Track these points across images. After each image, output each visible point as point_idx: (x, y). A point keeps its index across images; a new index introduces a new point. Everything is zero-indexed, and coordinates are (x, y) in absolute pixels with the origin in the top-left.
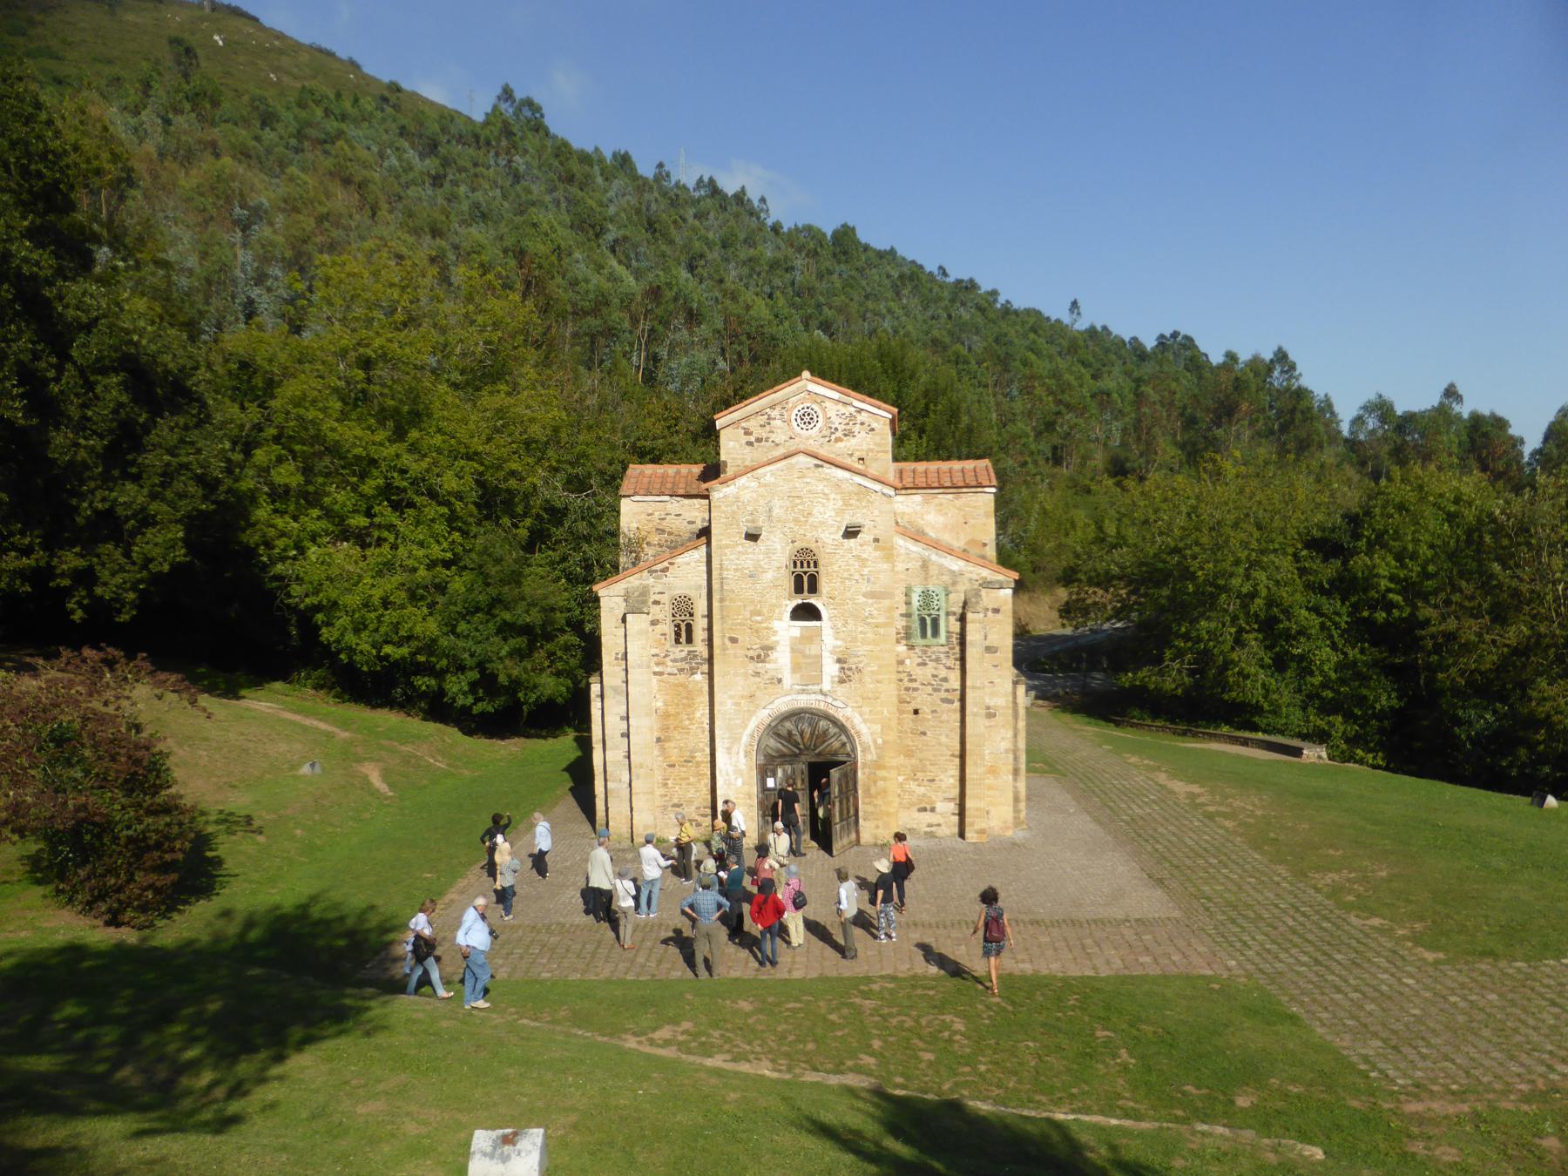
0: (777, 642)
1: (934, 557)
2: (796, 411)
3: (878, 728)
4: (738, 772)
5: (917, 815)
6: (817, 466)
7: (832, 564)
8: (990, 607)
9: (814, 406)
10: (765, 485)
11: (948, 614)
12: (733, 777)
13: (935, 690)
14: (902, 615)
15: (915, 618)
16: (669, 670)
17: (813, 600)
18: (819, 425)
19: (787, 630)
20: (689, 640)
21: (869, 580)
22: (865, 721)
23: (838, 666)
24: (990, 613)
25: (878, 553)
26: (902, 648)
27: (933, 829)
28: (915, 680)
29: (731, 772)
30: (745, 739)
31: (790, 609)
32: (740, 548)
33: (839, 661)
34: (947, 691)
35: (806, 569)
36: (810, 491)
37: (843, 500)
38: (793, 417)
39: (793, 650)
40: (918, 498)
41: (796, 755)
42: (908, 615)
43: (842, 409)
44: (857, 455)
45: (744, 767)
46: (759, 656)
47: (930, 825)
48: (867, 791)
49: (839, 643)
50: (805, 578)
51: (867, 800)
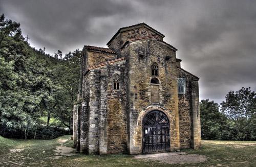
16: (112, 97)
17: (157, 77)
19: (150, 87)
20: (118, 88)
33: (164, 96)
43: (153, 33)
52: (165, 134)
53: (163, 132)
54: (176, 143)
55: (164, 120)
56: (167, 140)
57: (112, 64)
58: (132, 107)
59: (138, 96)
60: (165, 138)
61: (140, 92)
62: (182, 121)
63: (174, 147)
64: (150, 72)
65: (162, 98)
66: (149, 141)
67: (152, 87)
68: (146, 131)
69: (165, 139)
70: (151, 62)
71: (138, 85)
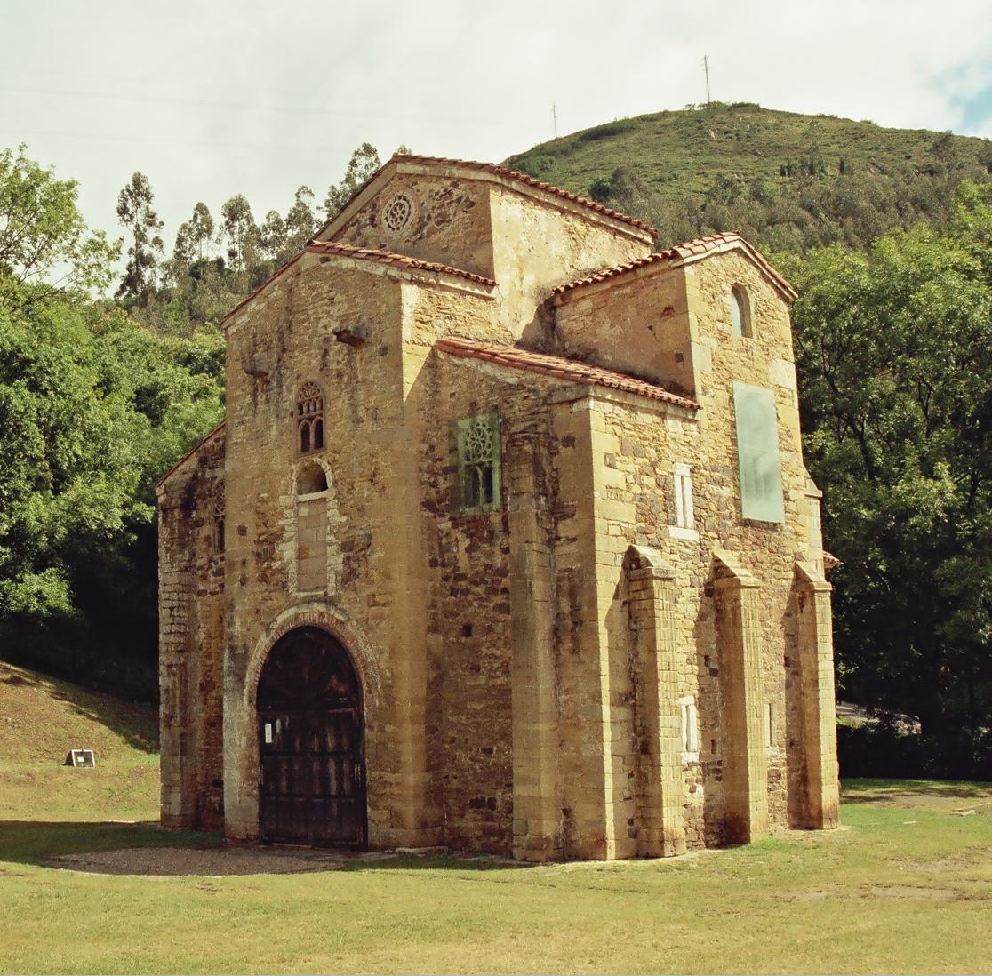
2: (387, 207)
8: (562, 435)
11: (503, 459)
12: (237, 733)
13: (493, 591)
16: (212, 587)
17: (316, 459)
18: (410, 220)
26: (445, 525)
28: (462, 577)
31: (294, 478)
34: (505, 591)
35: (313, 414)
38: (383, 217)
40: (586, 305)
42: (453, 469)
43: (437, 187)
46: (265, 550)
49: (344, 519)
50: (312, 430)
52: (338, 754)
53: (331, 742)
54: (398, 806)
56: (346, 785)
57: (211, 442)
58: (231, 624)
59: (252, 570)
61: (254, 548)
62: (482, 679)
63: (385, 828)
65: (336, 561)
67: (304, 511)
70: (295, 388)
71: (249, 520)
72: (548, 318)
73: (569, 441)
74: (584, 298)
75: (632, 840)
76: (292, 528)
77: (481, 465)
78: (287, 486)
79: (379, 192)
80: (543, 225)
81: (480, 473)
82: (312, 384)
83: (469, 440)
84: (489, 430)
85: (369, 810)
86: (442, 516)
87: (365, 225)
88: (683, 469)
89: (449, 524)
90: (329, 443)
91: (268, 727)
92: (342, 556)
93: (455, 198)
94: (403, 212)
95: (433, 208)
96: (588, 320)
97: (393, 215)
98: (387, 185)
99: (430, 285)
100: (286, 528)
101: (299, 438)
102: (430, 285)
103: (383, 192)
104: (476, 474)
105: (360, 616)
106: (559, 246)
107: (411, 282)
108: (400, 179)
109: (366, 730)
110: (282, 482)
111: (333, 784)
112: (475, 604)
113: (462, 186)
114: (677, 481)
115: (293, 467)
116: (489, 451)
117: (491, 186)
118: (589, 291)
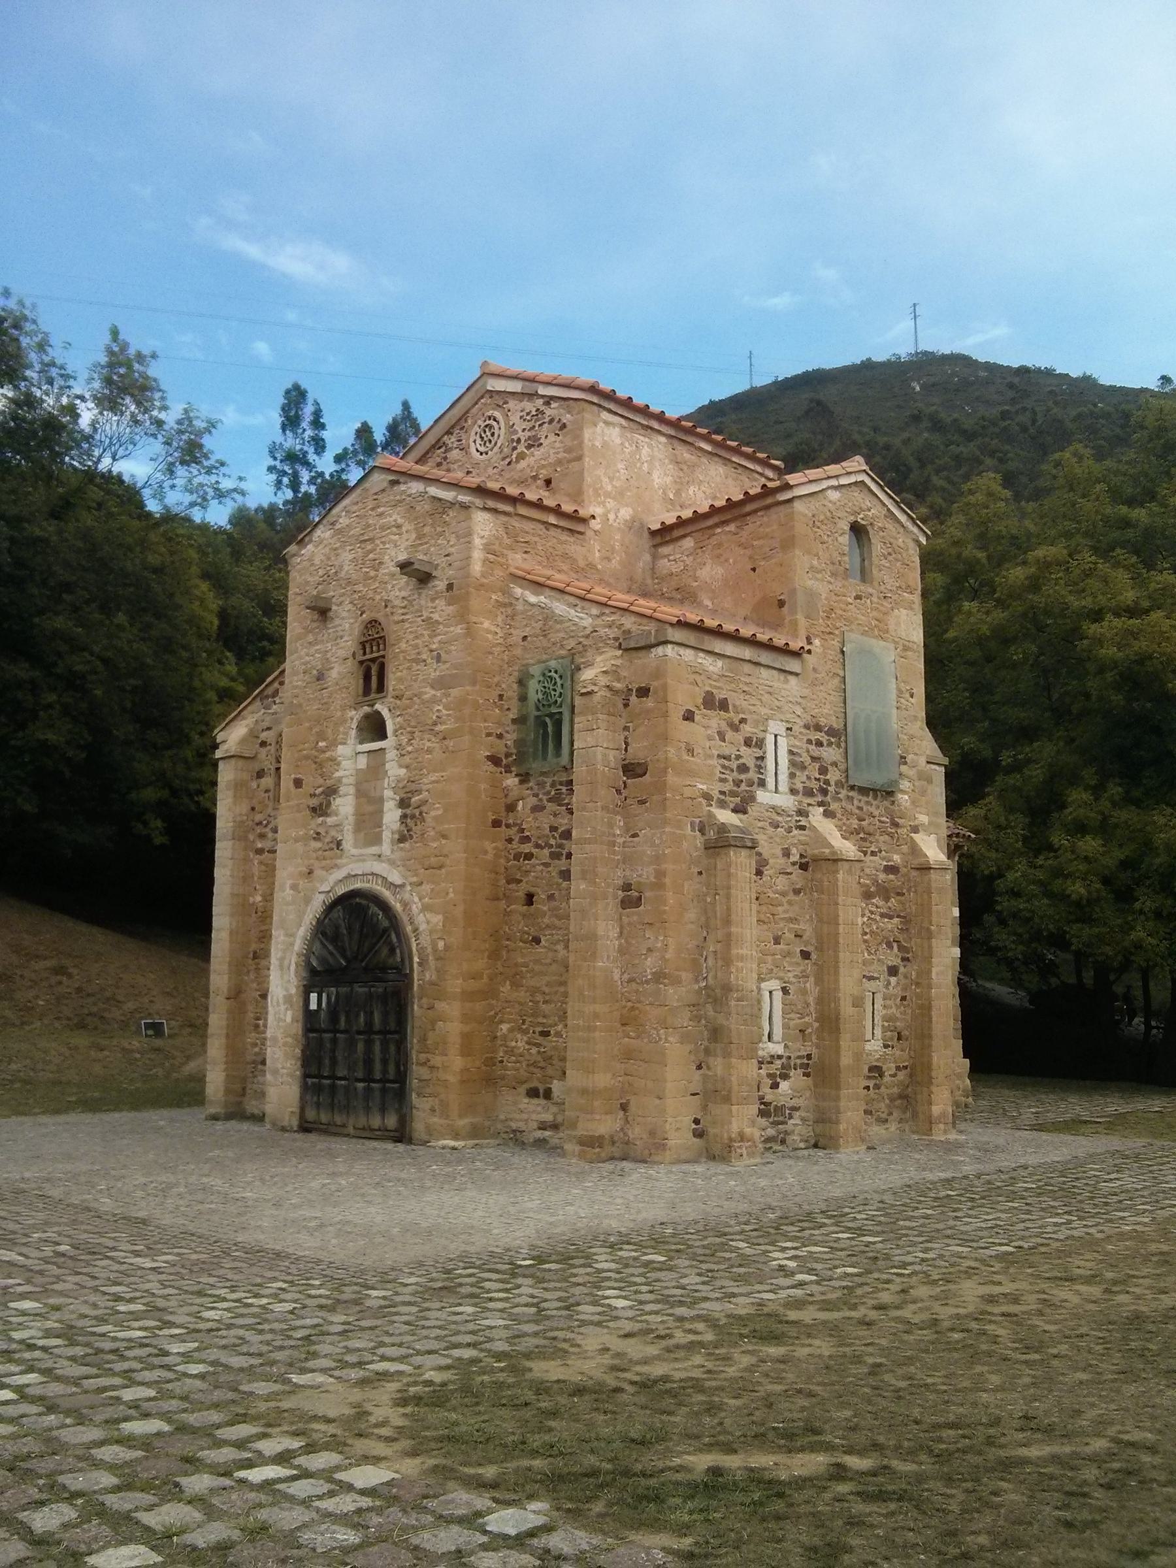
0: (339, 780)
1: (560, 607)
2: (476, 428)
3: (437, 919)
4: (288, 999)
5: (525, 1102)
6: (394, 483)
7: (399, 640)
8: (635, 686)
9: (497, 414)
10: (340, 531)
12: (283, 1007)
13: (555, 856)
14: (514, 721)
15: (531, 720)
17: (378, 707)
18: (499, 445)
21: (438, 659)
22: (426, 908)
23: (399, 812)
24: (633, 699)
25: (451, 609)
26: (511, 781)
27: (547, 1133)
28: (526, 839)
29: (281, 1001)
30: (299, 945)
31: (354, 726)
32: (310, 638)
33: (403, 803)
35: (375, 655)
36: (383, 528)
37: (416, 529)
39: (360, 794)
40: (688, 543)
41: (344, 970)
42: (520, 721)
43: (529, 406)
44: (544, 474)
45: (293, 991)
46: (321, 804)
47: (543, 1126)
48: (423, 1039)
49: (403, 771)
50: (374, 672)
51: (423, 1056)
55: (385, 952)
56: (391, 1069)
60: (385, 1049)
64: (357, 684)
66: (320, 1064)
68: (313, 1006)
69: (385, 1062)
72: (647, 557)
73: (643, 692)
74: (684, 536)
75: (695, 1140)
76: (352, 780)
77: (551, 715)
78: (346, 734)
79: (467, 412)
80: (645, 451)
81: (550, 729)
82: (376, 621)
83: (540, 687)
84: (561, 677)
85: (414, 1095)
86: (508, 771)
87: (451, 449)
88: (777, 727)
89: (517, 780)
90: (391, 689)
91: (314, 997)
92: (399, 812)
93: (547, 420)
94: (493, 435)
95: (524, 430)
96: (689, 560)
97: (482, 438)
98: (476, 403)
99: (505, 513)
100: (345, 780)
101: (361, 681)
102: (505, 513)
103: (474, 410)
104: (545, 725)
105: (415, 879)
106: (661, 477)
107: (485, 509)
108: (491, 397)
109: (416, 1007)
110: (341, 729)
111: (378, 1066)
112: (540, 868)
113: (554, 405)
114: (770, 739)
115: (354, 712)
116: (559, 700)
117: (586, 405)
118: (689, 529)
